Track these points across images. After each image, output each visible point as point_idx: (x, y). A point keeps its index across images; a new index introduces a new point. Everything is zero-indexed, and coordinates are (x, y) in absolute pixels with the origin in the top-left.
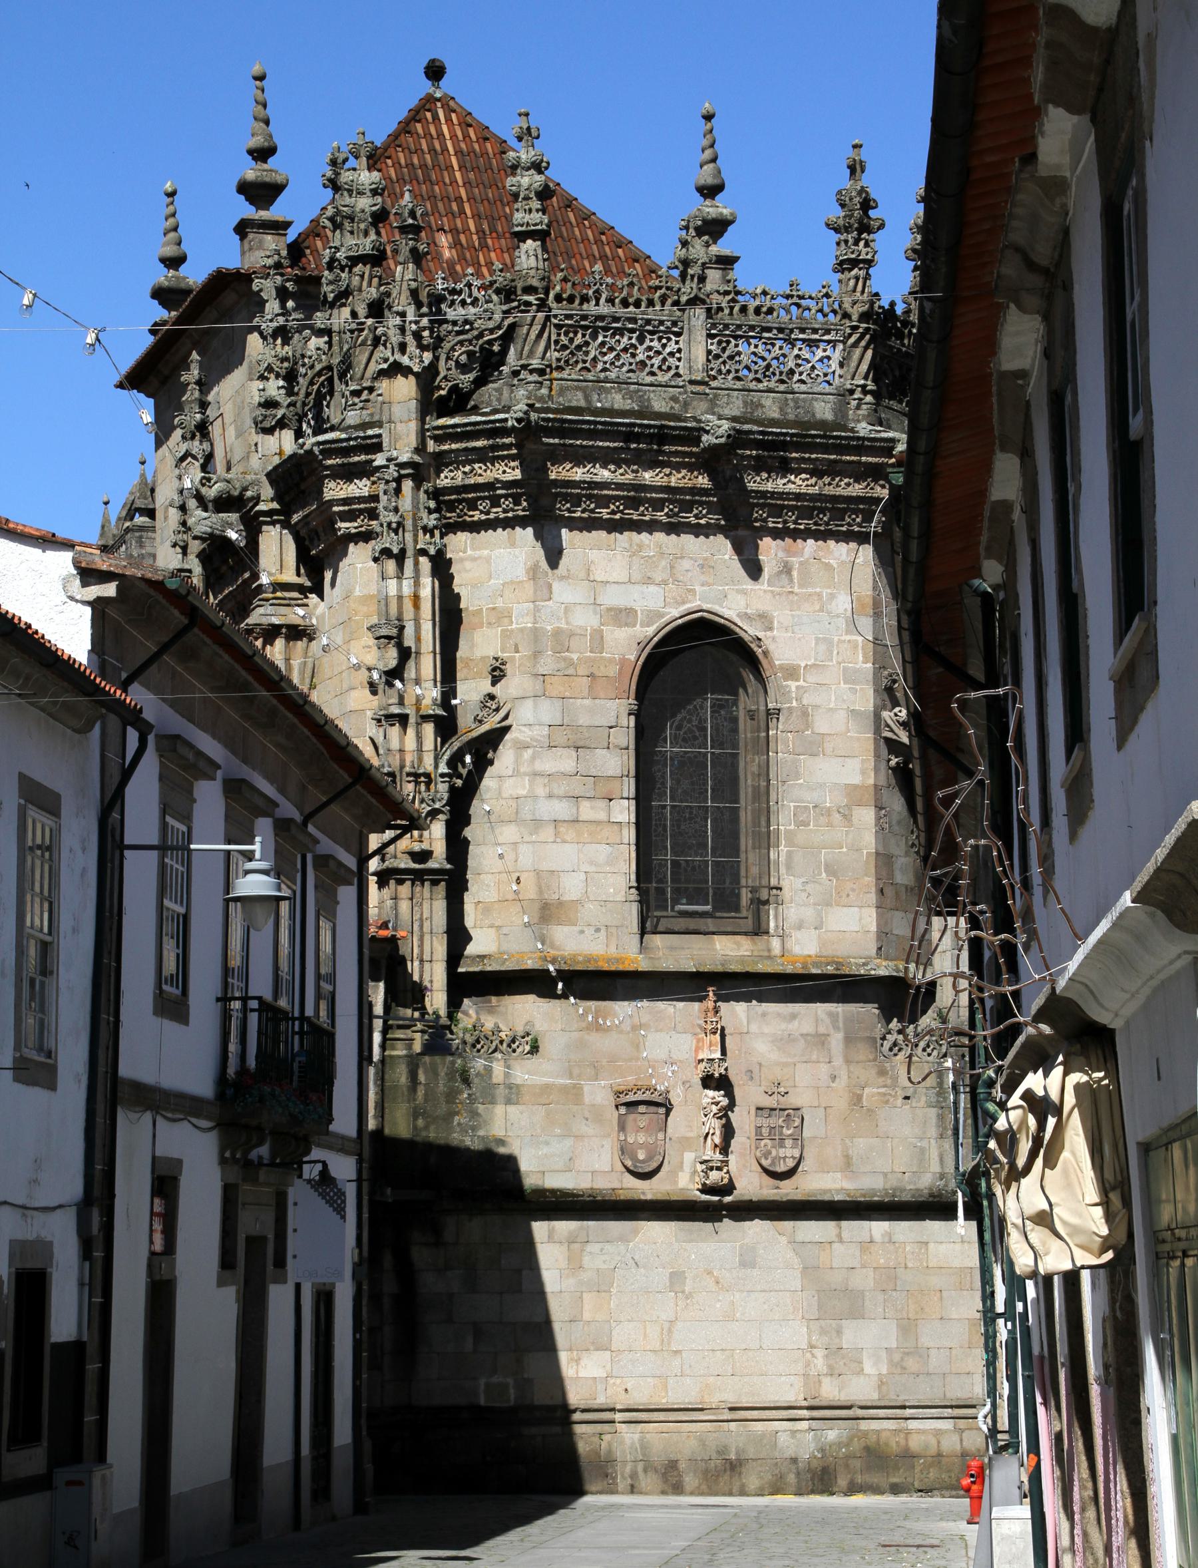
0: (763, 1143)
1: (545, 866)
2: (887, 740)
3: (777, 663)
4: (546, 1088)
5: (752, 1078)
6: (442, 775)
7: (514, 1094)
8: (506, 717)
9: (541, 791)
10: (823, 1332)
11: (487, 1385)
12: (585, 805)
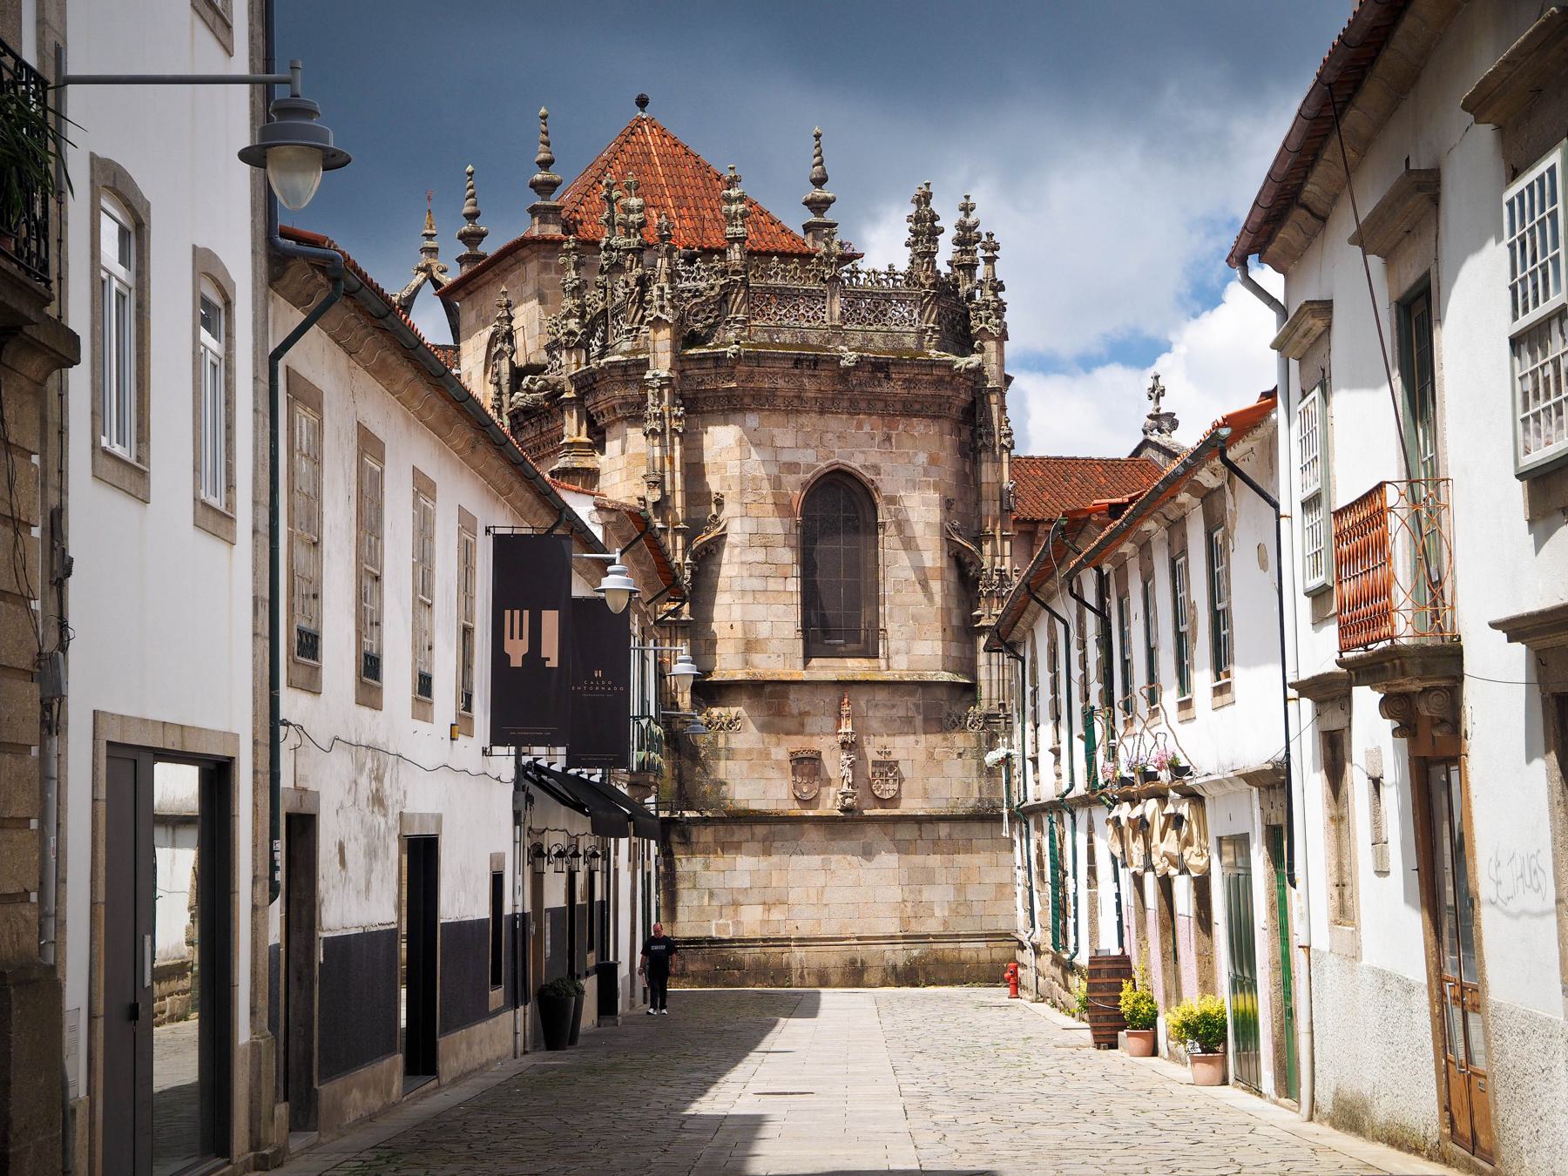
2: (947, 539)
4: (750, 751)
6: (687, 564)
7: (731, 754)
9: (746, 574)
10: (911, 892)
11: (716, 924)
12: (771, 580)
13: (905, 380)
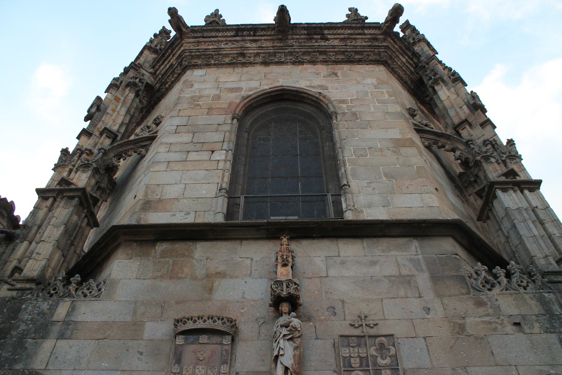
1: (154, 182)
3: (332, 99)
5: (335, 314)
8: (156, 132)
13: (342, 40)
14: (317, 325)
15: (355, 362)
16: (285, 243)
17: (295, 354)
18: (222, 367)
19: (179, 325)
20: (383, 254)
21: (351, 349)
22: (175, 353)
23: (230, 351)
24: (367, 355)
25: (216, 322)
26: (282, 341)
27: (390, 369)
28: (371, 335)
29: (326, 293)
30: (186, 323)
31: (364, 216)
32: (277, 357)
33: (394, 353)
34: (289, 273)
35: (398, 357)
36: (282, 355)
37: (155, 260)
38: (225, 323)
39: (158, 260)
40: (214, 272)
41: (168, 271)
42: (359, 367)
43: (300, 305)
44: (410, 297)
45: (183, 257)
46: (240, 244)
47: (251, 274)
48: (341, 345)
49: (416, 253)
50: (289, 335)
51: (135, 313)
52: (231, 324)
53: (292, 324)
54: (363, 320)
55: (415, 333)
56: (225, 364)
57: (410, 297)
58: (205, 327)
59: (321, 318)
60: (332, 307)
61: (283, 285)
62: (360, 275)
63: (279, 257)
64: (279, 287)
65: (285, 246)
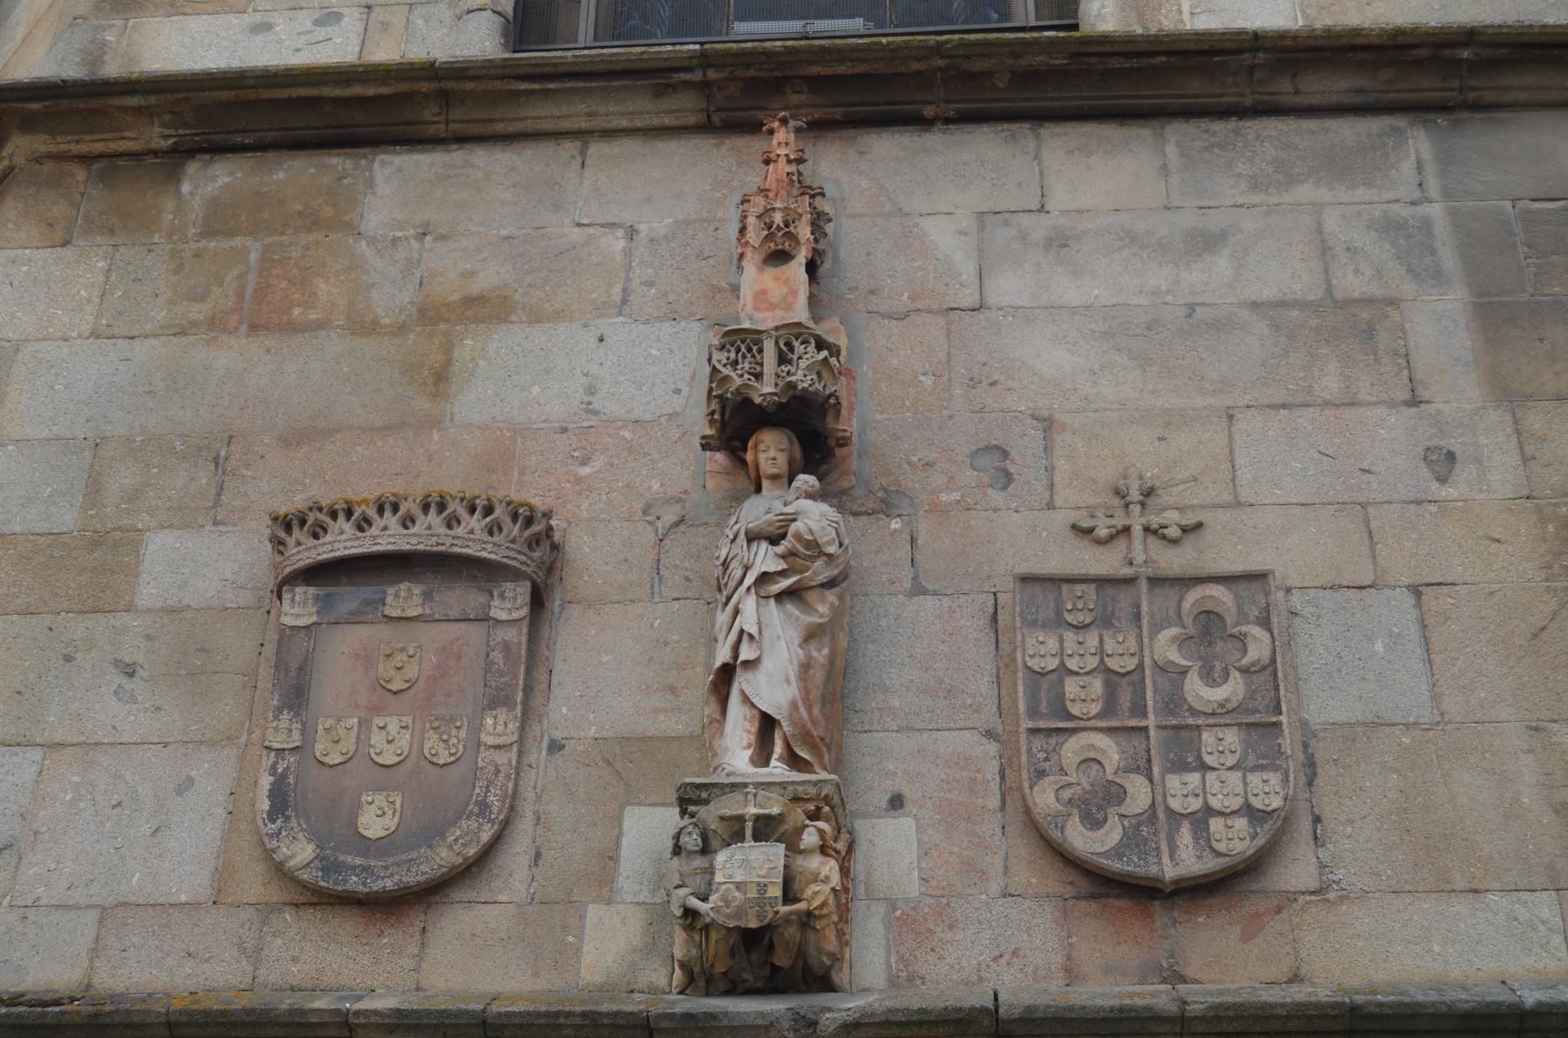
0: (1071, 749)
14: (924, 528)
15: (1084, 695)
16: (782, 151)
17: (809, 657)
18: (489, 721)
19: (291, 541)
20: (1255, 199)
21: (1069, 636)
22: (280, 665)
23: (523, 652)
24: (1141, 666)
25: (459, 522)
26: (750, 604)
27: (1239, 725)
28: (1160, 574)
29: (973, 383)
30: (325, 530)
31: (1180, 12)
32: (726, 675)
33: (1266, 654)
34: (793, 293)
35: (1280, 675)
36: (748, 664)
37: (180, 246)
38: (500, 529)
39: (193, 246)
40: (456, 297)
41: (240, 296)
42: (1097, 717)
43: (844, 442)
44: (1369, 404)
45: (309, 231)
46: (579, 160)
47: (624, 301)
48: (1024, 619)
49: (1417, 194)
50: (782, 574)
51: (94, 490)
52: (527, 533)
53: (793, 527)
54: (1136, 509)
55: (1375, 564)
56: (504, 704)
57: (1369, 404)
58: (409, 547)
59: (944, 497)
60: (997, 447)
61: (760, 351)
62: (1135, 301)
63: (751, 220)
64: (744, 357)
65: (783, 167)
